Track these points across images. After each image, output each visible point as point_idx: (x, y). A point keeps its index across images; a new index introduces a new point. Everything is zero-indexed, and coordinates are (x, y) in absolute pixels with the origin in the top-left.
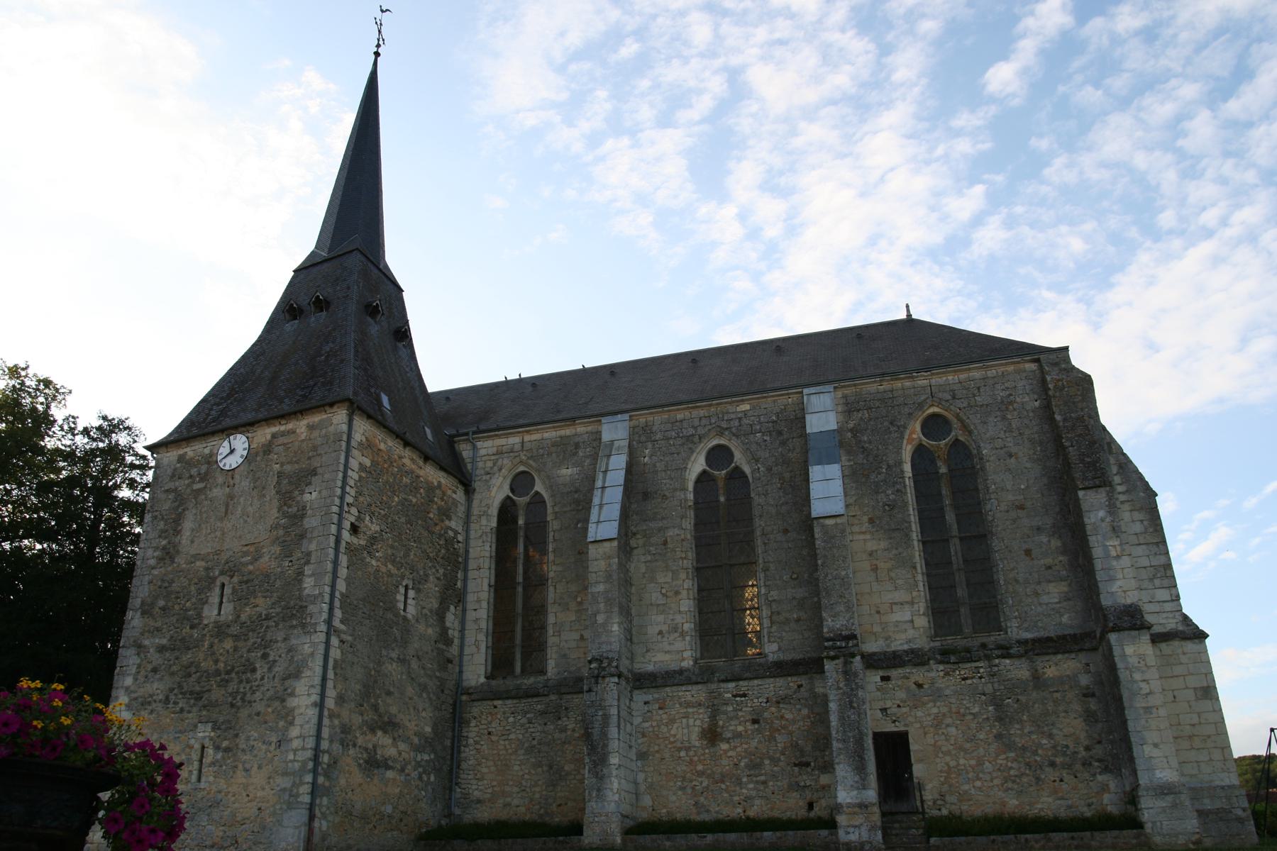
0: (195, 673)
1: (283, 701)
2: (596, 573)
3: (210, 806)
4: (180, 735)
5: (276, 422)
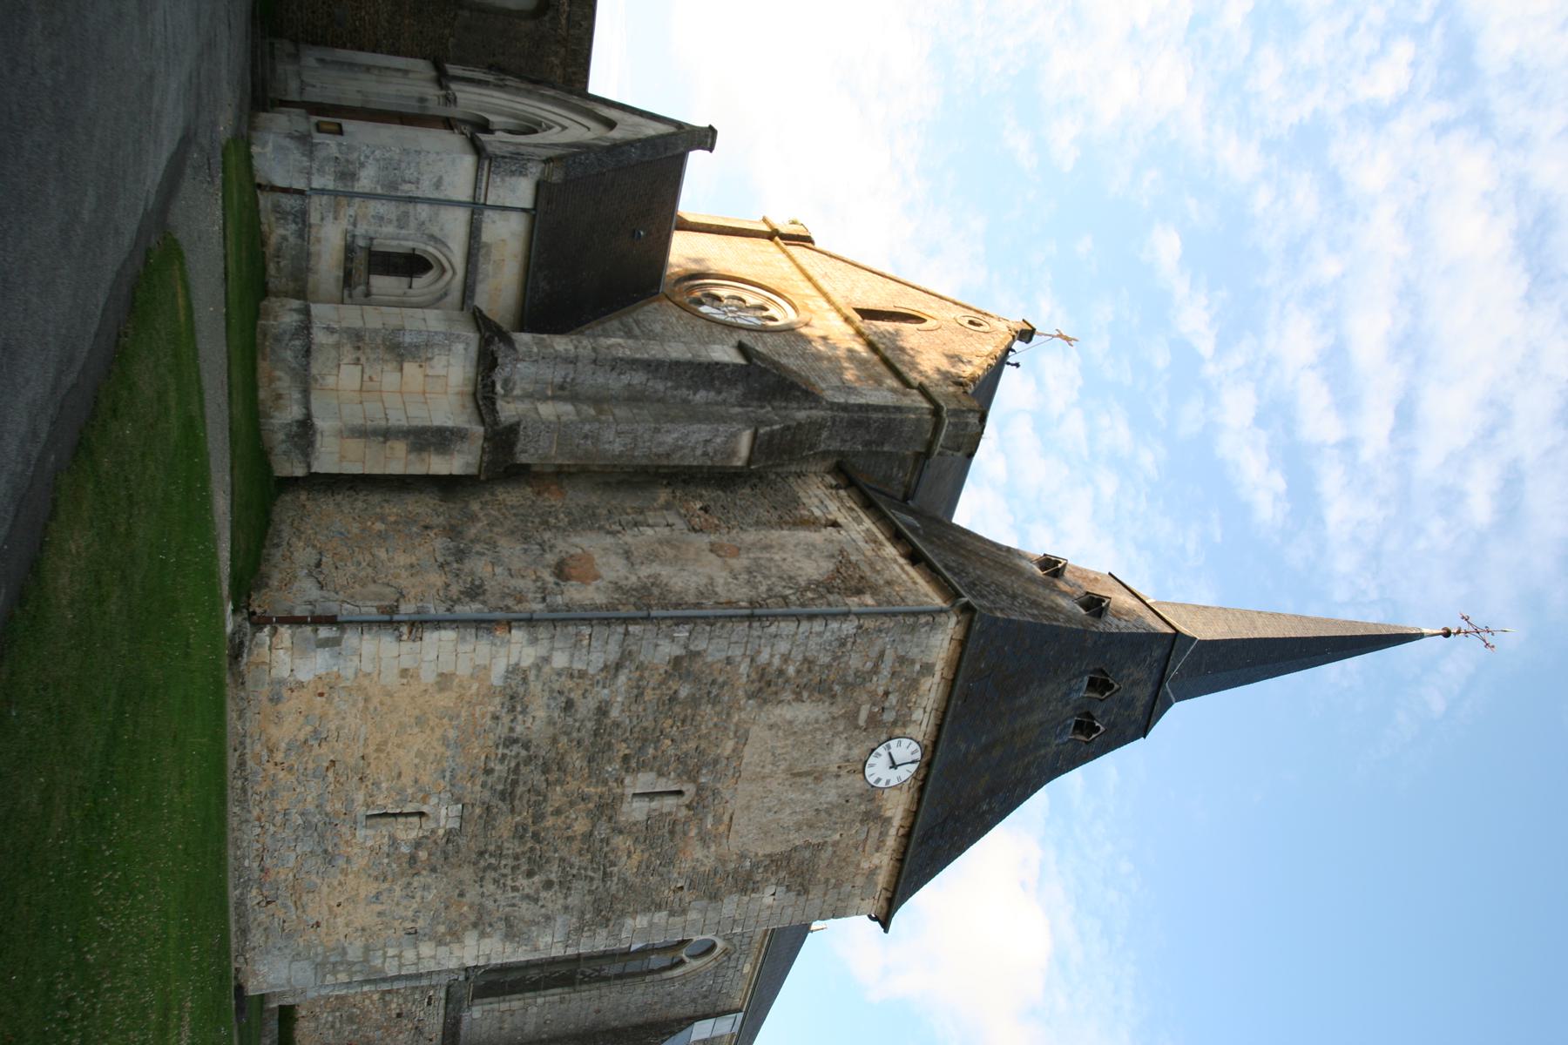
0: (547, 780)
1: (475, 925)
3: (326, 851)
4: (447, 779)
5: (907, 823)
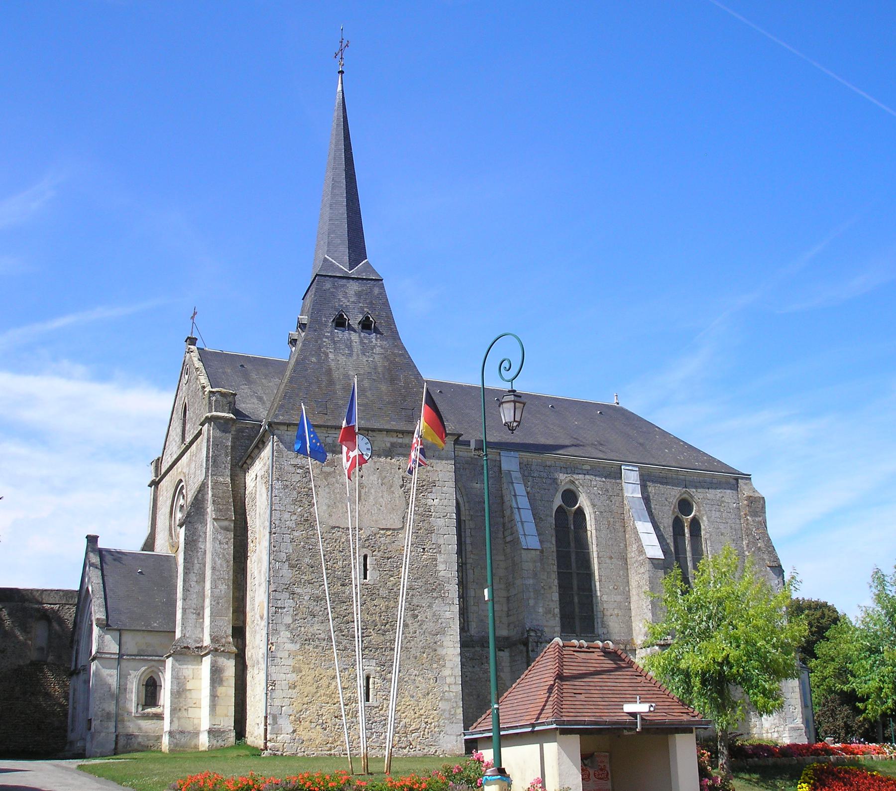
2: (527, 571)
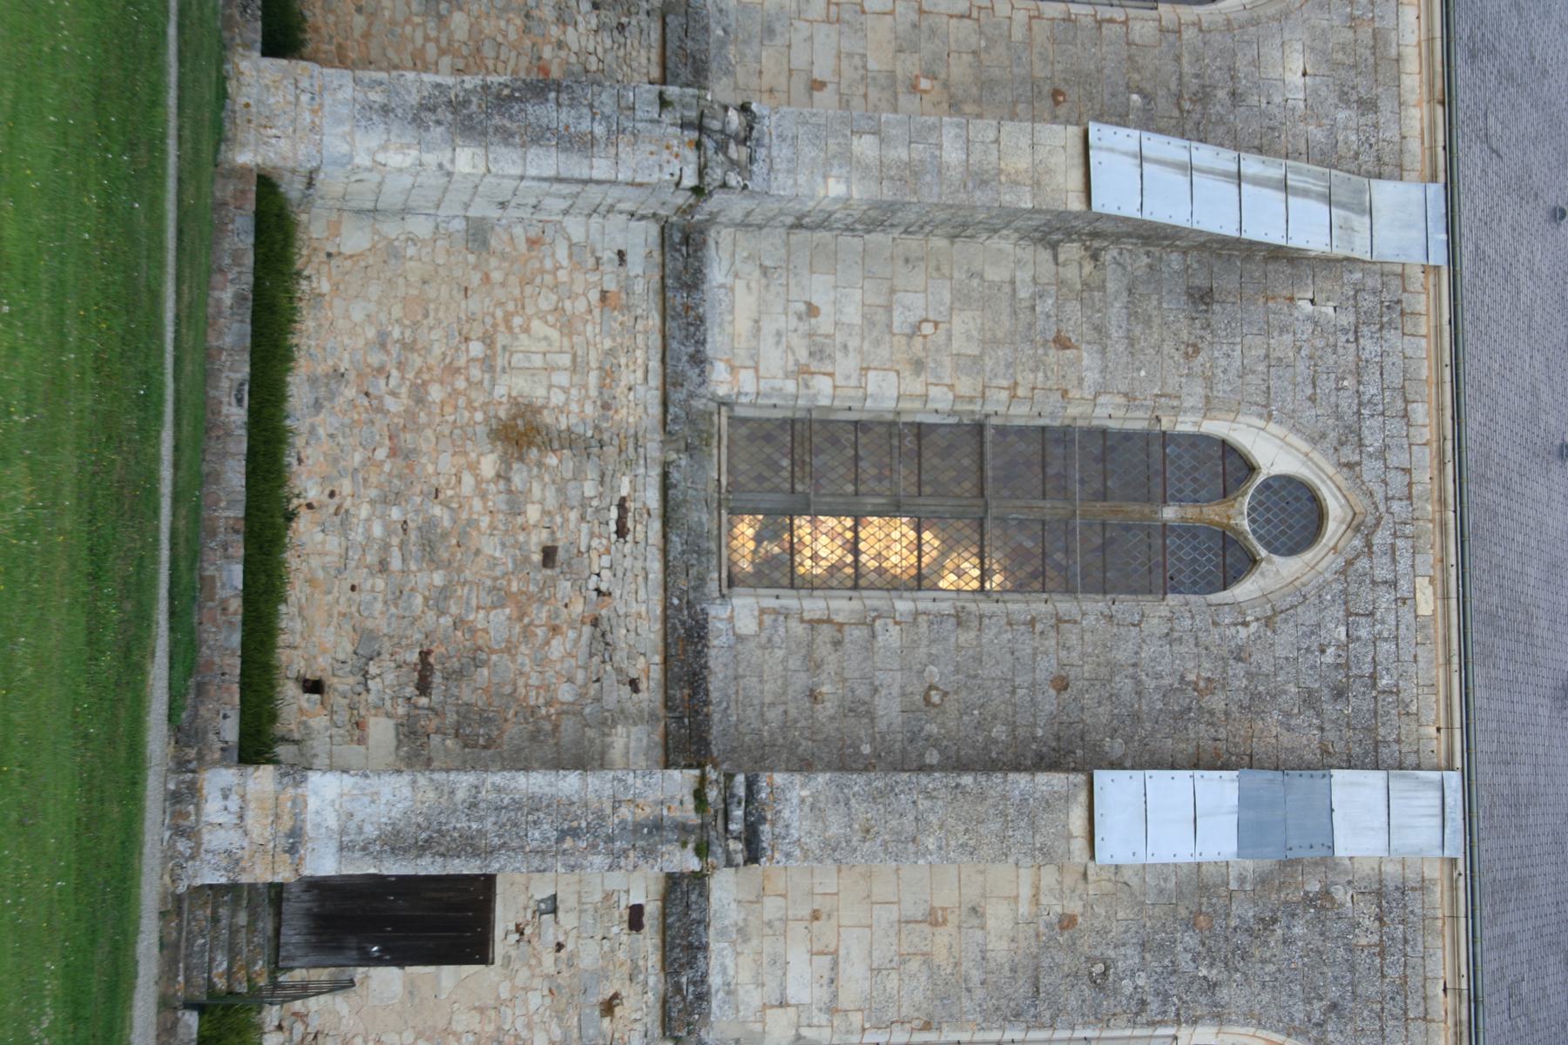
2: (997, 141)
